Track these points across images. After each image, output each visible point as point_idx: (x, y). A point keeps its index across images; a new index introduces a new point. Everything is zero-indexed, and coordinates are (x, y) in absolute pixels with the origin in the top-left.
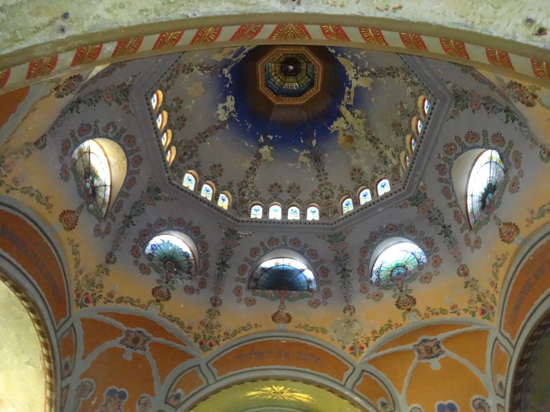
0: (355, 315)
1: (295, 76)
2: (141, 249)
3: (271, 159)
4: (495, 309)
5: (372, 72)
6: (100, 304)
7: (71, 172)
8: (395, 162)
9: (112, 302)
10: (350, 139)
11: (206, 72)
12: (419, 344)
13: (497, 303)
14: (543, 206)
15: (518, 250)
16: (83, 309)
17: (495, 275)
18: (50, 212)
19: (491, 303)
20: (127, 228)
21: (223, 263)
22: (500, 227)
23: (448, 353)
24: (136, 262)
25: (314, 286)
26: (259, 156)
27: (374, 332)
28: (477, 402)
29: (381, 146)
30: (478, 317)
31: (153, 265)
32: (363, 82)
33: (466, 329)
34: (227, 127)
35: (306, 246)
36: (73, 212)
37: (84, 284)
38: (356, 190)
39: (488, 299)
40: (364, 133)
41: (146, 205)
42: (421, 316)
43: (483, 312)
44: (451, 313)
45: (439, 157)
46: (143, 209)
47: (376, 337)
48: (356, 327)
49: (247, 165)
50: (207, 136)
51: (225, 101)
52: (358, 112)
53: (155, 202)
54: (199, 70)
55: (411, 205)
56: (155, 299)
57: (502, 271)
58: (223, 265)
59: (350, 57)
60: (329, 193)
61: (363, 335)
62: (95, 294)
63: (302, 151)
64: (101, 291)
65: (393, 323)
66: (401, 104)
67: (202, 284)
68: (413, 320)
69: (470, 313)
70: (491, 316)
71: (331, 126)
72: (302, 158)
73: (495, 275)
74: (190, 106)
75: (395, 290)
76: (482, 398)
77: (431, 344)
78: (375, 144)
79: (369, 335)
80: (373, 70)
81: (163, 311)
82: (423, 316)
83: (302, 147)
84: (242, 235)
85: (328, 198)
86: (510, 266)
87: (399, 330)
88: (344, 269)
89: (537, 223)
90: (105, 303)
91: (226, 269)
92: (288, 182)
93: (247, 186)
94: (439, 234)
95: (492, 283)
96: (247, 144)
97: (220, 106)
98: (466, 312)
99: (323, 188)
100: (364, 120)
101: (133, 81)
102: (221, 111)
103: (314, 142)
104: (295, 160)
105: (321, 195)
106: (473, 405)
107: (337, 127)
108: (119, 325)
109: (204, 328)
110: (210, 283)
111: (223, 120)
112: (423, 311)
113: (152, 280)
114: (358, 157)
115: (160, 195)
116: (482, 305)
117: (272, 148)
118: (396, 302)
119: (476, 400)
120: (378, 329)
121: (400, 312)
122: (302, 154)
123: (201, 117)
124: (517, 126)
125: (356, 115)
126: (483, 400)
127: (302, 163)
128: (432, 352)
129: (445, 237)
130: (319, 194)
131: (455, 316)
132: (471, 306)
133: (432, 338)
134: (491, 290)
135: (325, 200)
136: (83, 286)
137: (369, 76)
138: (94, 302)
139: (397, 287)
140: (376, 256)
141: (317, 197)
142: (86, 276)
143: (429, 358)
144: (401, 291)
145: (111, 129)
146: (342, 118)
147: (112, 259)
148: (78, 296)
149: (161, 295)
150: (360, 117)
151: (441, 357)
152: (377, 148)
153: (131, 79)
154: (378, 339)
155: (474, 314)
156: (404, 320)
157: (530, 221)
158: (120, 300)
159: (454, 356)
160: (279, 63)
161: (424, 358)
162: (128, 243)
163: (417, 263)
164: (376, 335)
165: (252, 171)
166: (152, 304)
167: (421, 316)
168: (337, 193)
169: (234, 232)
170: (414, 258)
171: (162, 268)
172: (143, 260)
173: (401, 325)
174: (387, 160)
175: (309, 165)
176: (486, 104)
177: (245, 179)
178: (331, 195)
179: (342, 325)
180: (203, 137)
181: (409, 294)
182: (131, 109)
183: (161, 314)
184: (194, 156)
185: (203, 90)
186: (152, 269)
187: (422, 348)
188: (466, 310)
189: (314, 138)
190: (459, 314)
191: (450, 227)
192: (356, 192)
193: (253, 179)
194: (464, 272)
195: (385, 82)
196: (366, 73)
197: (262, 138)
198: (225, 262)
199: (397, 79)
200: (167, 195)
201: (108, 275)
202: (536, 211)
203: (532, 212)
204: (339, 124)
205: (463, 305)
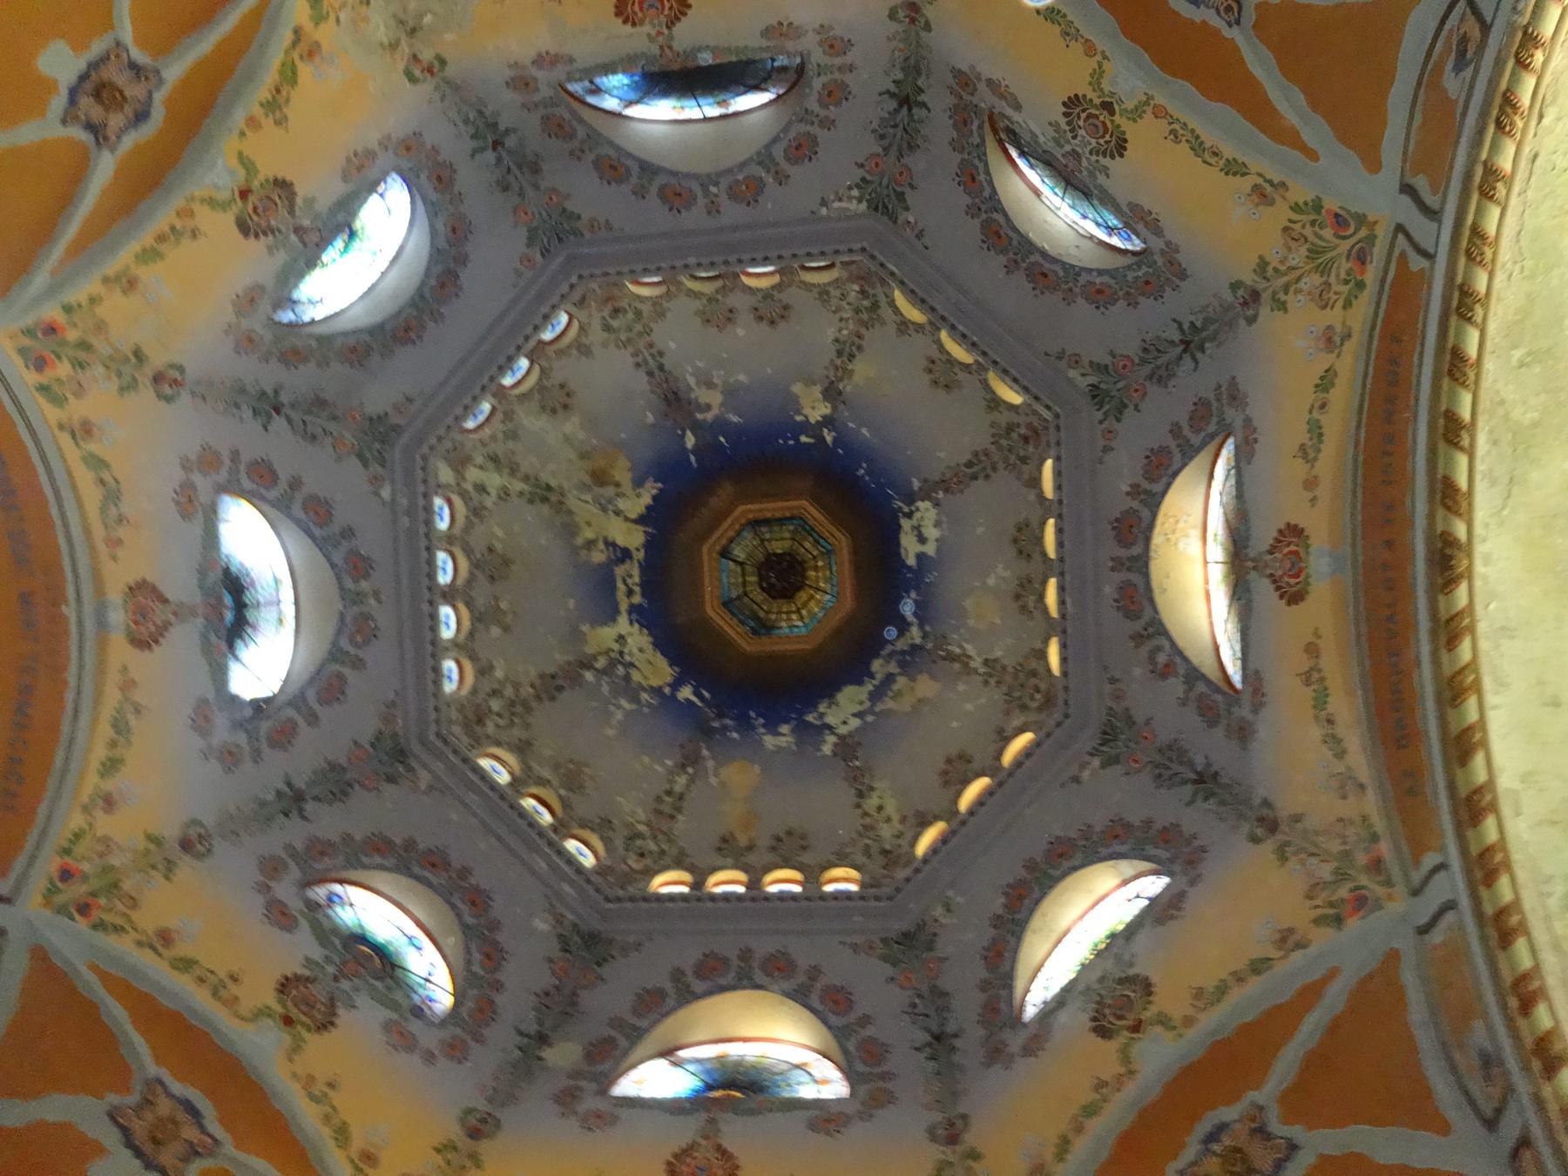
0: (401, 66)
3: (797, 388)
4: (32, 377)
5: (589, 667)
8: (473, 474)
9: (1260, 175)
10: (600, 478)
11: (958, 651)
13: (41, 400)
15: (100, 591)
17: (97, 463)
18: (1317, 634)
20: (1198, 324)
23: (47, 128)
26: (832, 393)
27: (312, 52)
29: (519, 486)
30: (51, 312)
32: (605, 636)
33: (58, 251)
34: (916, 484)
35: (640, 193)
39: (63, 369)
40: (572, 502)
41: (1137, 360)
42: (203, 201)
43: (51, 329)
45: (376, 594)
46: (1145, 350)
47: (295, 44)
48: (379, 27)
49: (862, 369)
50: (969, 464)
51: (921, 557)
52: (599, 556)
53: (1108, 360)
54: (970, 657)
57: (92, 496)
59: (644, 696)
60: (615, 324)
61: (342, 16)
62: (1313, 223)
63: (717, 418)
64: (1290, 221)
65: (267, 123)
66: (506, 629)
68: (217, 173)
70: (26, 342)
71: (654, 492)
72: (714, 398)
73: (97, 463)
74: (1000, 569)
77: (116, 121)
78: (537, 486)
79: (325, 34)
80: (589, 676)
81: (1093, 63)
83: (720, 425)
84: (850, 198)
85: (616, 311)
86: (87, 531)
87: (239, 117)
88: (496, 144)
89: (112, 696)
90: (1283, 184)
91: (893, 88)
92: (741, 332)
93: (857, 311)
95: (86, 430)
96: (864, 431)
97: (930, 549)
99: (638, 327)
100: (579, 541)
101: (1083, 766)
102: (932, 533)
103: (690, 441)
104: (730, 392)
105: (638, 313)
107: (638, 496)
108: (1258, 62)
111: (927, 504)
114: (567, 439)
115: (1092, 380)
117: (799, 418)
120: (305, 71)
121: (268, 168)
122: (715, 412)
123: (980, 530)
125: (601, 546)
127: (710, 385)
128: (97, 95)
131: (113, 266)
133: (128, 142)
134: (78, 409)
136: (1343, 276)
137: (595, 658)
138: (1317, 206)
140: (417, 223)
141: (646, 309)
143: (94, 66)
144: (298, 230)
145: (1162, 659)
146: (633, 516)
148: (1362, 258)
150: (590, 544)
151: (58, 103)
152: (526, 479)
153: (1086, 774)
154: (288, 36)
155: (68, 309)
156: (240, 154)
157: (128, 685)
159: (28, 133)
161: (104, 59)
165: (847, 351)
167: (203, 201)
168: (596, 335)
169: (878, 206)
173: (243, 134)
174: (490, 465)
175: (692, 381)
177: (863, 331)
179: (428, 19)
185: (968, 603)
187: (134, 91)
188: (93, 300)
189: (694, 452)
190: (106, 280)
193: (840, 330)
194: (167, 382)
195: (557, 656)
196: (601, 663)
197: (829, 439)
198: (901, 106)
199: (533, 673)
200: (1072, 373)
202: (132, 720)
203: (138, 711)
204: (638, 502)
205: (115, 307)
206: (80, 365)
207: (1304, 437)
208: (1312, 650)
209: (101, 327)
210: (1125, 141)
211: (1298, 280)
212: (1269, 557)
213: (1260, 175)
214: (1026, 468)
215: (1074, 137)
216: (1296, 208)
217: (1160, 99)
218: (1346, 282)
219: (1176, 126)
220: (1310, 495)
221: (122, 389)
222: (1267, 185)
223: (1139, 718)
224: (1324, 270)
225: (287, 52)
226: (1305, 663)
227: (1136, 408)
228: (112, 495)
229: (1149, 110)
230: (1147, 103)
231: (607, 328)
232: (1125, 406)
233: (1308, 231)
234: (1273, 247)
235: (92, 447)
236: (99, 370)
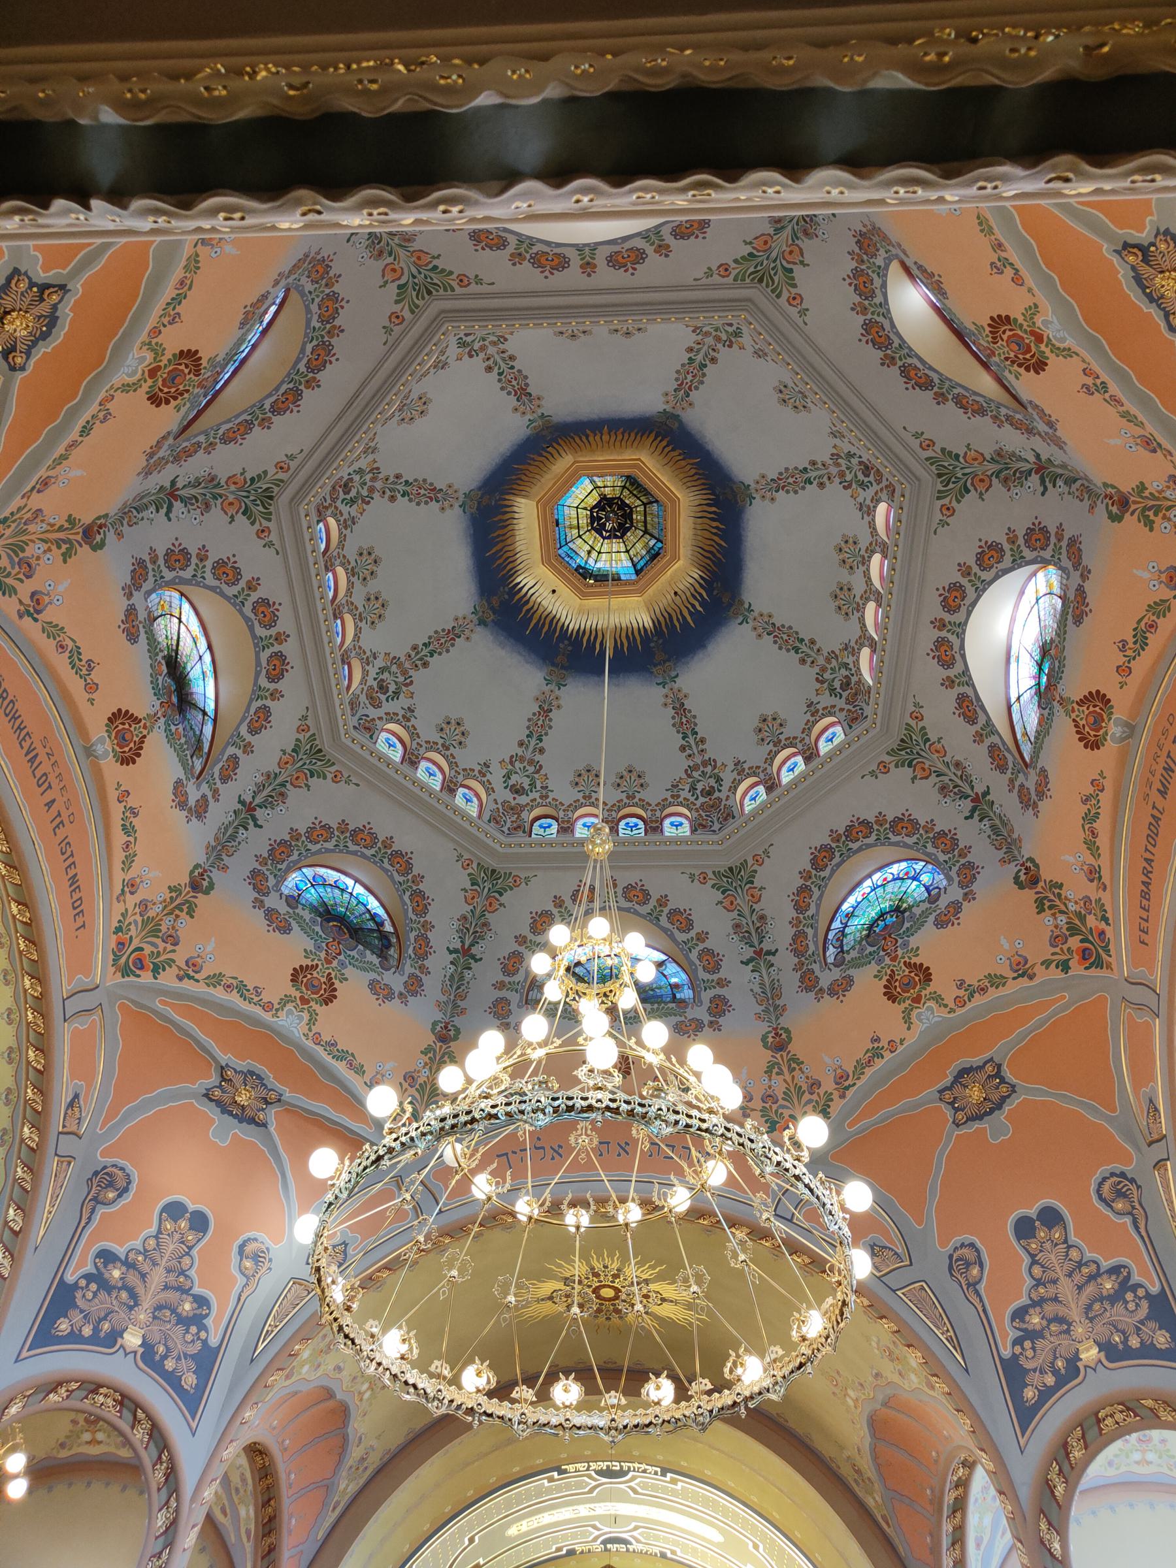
1: (622, 537)
2: (272, 882)
6: (168, 979)
7: (142, 630)
9: (198, 981)
12: (952, 1083)
14: (1139, 622)
16: (127, 979)
18: (91, 701)
19: (1097, 923)
20: (242, 830)
21: (466, 952)
22: (1073, 716)
24: (258, 903)
25: (686, 994)
28: (1107, 1186)
31: (299, 919)
36: (137, 720)
37: (136, 922)
38: (770, 759)
42: (946, 1006)
43: (1084, 954)
44: (1014, 978)
47: (847, 1088)
55: (897, 766)
56: (298, 995)
58: (465, 955)
60: (712, 782)
64: (174, 951)
65: (884, 1043)
67: (414, 986)
69: (1057, 967)
70: (1104, 956)
73: (1092, 847)
75: (880, 961)
76: (1118, 1167)
79: (828, 1085)
82: (952, 1005)
85: (709, 793)
90: (180, 979)
91: (473, 964)
94: (966, 818)
95: (1094, 874)
98: (1047, 968)
99: (696, 774)
105: (693, 789)
106: (1100, 1197)
109: (413, 1091)
110: (433, 985)
112: (950, 994)
113: (297, 947)
116: (1082, 941)
118: (885, 987)
119: (1104, 1179)
124: (1066, 489)
126: (1123, 1175)
129: (980, 821)
130: (687, 787)
131: (1024, 982)
132: (1057, 950)
134: (1091, 890)
135: (702, 799)
136: (132, 927)
138: (156, 970)
139: (882, 953)
141: (685, 794)
142: (144, 905)
144: (894, 959)
147: (205, 884)
149: (312, 986)
154: (850, 1094)
155: (1065, 966)
156: (909, 1028)
158: (215, 980)
160: (585, 509)
162: (242, 862)
163: (926, 895)
164: (847, 1084)
166: (290, 1006)
167: (946, 1006)
168: (728, 777)
170: (917, 886)
171: (318, 929)
172: (272, 901)
173: (902, 1041)
176: (1000, 471)
178: (716, 786)
180: (424, 654)
181: (917, 960)
182: (274, 537)
183: (311, 1034)
184: (402, 696)
186: (294, 924)
188: (1047, 963)
190: (1031, 978)
191: (987, 793)
192: (771, 765)
194: (1029, 877)
201: (192, 917)
202: (1131, 640)
206: (1082, 918)
207: (135, 821)
208: (91, 687)
209: (1055, 940)
210: (292, 980)
211: (165, 907)
212: (145, 732)
213: (198, 981)
214: (380, 663)
215: (330, 974)
216: (170, 962)
217: (267, 1017)
218: (130, 924)
219: (256, 999)
220: (123, 788)
221: (1061, 886)
222: (192, 974)
223: (241, 519)
224: (145, 923)
225: (854, 1084)
226: (95, 676)
227: (284, 752)
228: (1090, 818)
229: (277, 1006)
230: (277, 1010)
231: (719, 780)
232: (293, 751)
233: (161, 945)
234: (185, 925)
235: (1091, 860)
236: (1072, 907)
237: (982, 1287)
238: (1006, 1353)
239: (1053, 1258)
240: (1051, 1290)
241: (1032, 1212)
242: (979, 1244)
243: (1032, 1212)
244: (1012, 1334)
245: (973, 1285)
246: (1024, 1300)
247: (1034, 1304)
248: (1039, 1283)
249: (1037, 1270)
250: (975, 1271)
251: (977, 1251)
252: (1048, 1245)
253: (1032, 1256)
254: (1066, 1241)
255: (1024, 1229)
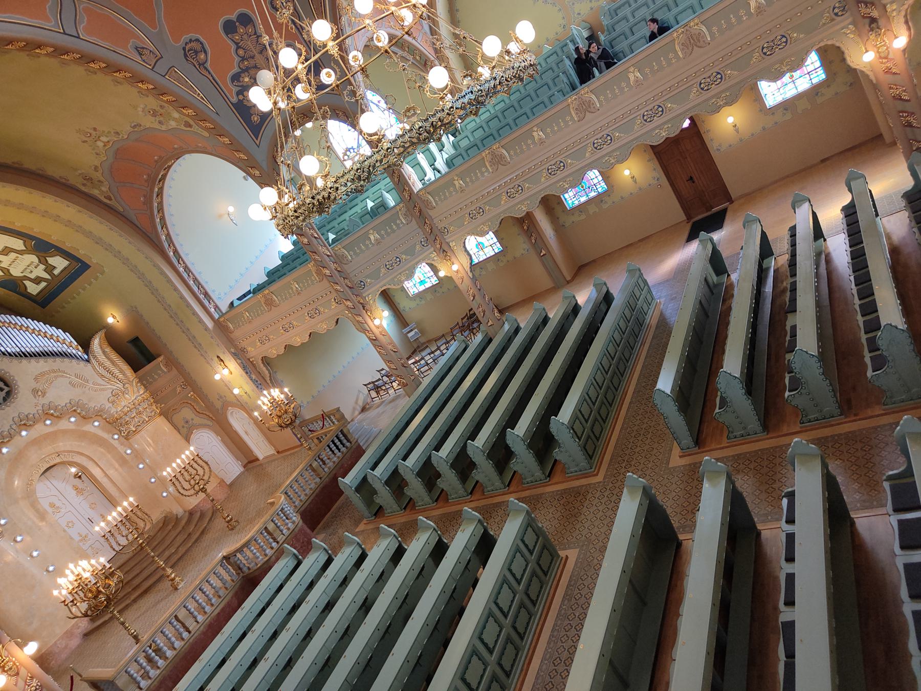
237: (208, 65)
238: (234, 100)
239: (249, 44)
240: (252, 62)
241: (233, 17)
242: (202, 39)
243: (233, 17)
244: (235, 90)
245: (202, 64)
246: (236, 70)
247: (243, 71)
248: (243, 59)
249: (241, 52)
250: (202, 56)
251: (201, 43)
252: (245, 37)
253: (237, 44)
254: (255, 34)
255: (230, 28)
